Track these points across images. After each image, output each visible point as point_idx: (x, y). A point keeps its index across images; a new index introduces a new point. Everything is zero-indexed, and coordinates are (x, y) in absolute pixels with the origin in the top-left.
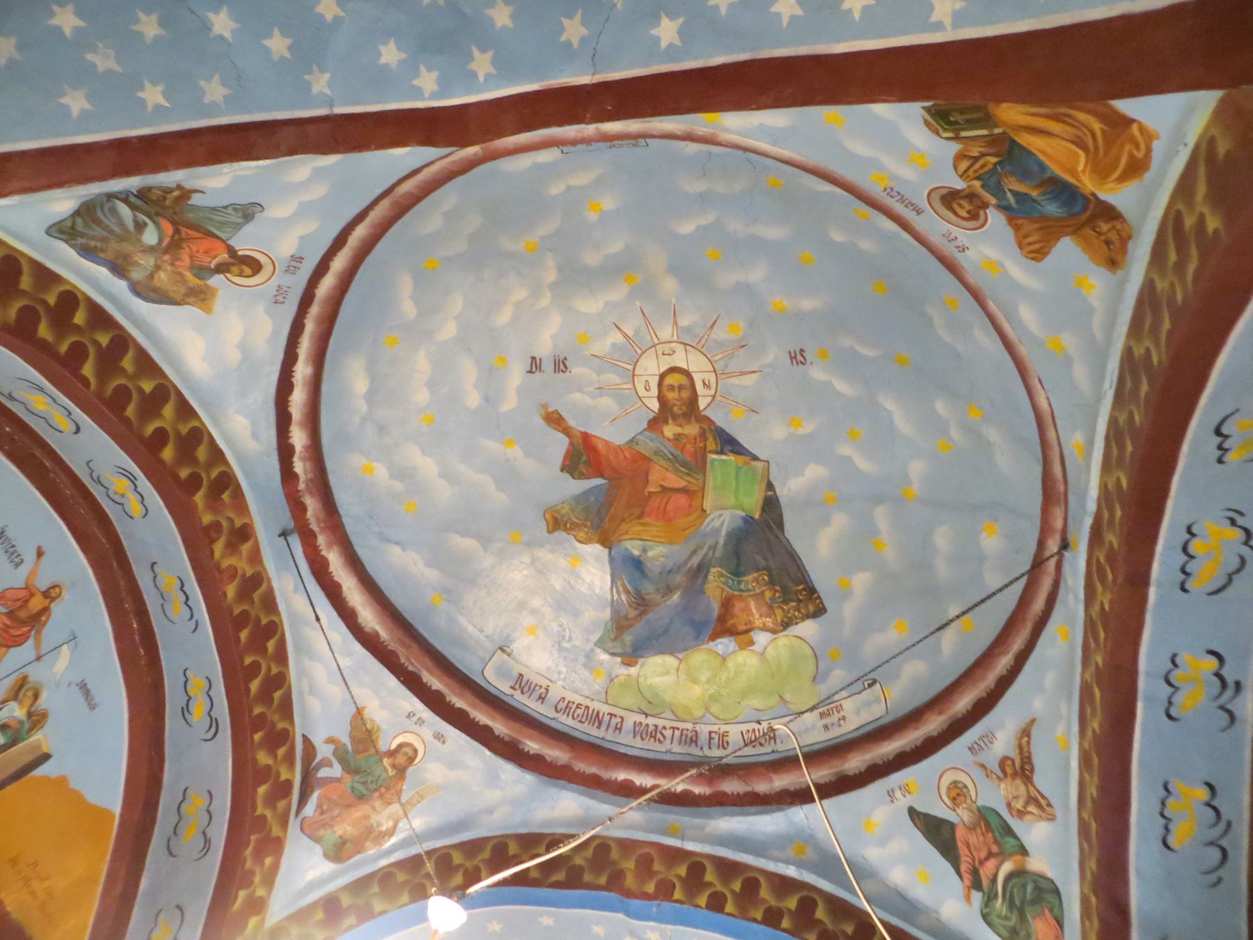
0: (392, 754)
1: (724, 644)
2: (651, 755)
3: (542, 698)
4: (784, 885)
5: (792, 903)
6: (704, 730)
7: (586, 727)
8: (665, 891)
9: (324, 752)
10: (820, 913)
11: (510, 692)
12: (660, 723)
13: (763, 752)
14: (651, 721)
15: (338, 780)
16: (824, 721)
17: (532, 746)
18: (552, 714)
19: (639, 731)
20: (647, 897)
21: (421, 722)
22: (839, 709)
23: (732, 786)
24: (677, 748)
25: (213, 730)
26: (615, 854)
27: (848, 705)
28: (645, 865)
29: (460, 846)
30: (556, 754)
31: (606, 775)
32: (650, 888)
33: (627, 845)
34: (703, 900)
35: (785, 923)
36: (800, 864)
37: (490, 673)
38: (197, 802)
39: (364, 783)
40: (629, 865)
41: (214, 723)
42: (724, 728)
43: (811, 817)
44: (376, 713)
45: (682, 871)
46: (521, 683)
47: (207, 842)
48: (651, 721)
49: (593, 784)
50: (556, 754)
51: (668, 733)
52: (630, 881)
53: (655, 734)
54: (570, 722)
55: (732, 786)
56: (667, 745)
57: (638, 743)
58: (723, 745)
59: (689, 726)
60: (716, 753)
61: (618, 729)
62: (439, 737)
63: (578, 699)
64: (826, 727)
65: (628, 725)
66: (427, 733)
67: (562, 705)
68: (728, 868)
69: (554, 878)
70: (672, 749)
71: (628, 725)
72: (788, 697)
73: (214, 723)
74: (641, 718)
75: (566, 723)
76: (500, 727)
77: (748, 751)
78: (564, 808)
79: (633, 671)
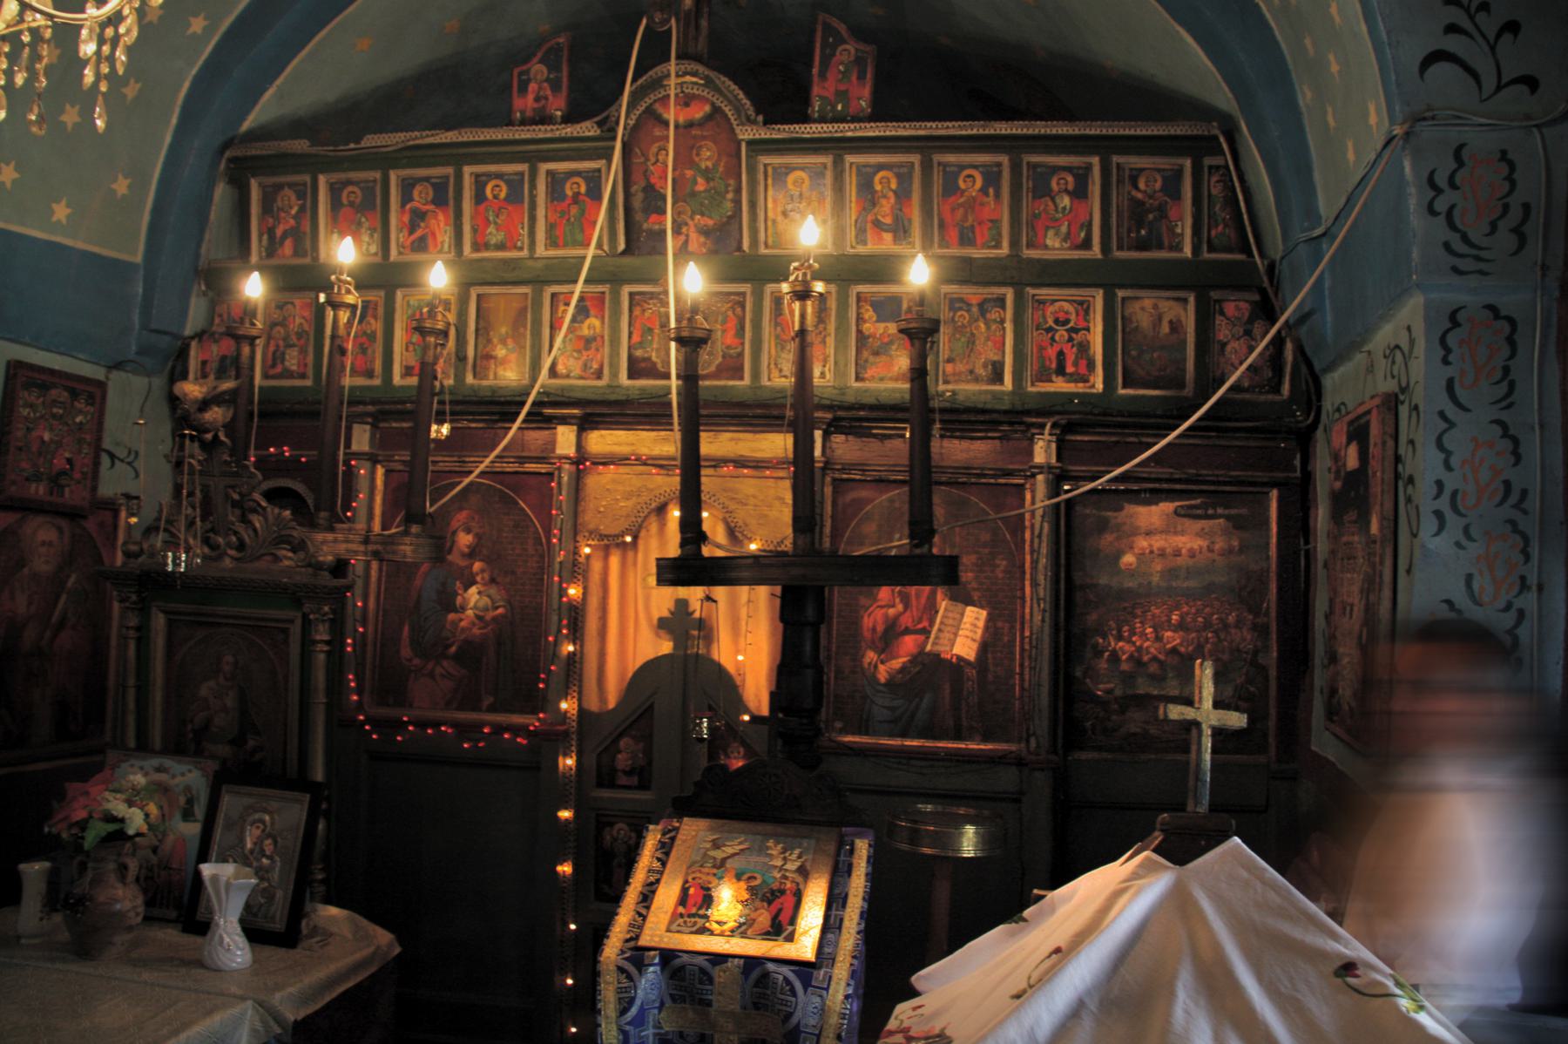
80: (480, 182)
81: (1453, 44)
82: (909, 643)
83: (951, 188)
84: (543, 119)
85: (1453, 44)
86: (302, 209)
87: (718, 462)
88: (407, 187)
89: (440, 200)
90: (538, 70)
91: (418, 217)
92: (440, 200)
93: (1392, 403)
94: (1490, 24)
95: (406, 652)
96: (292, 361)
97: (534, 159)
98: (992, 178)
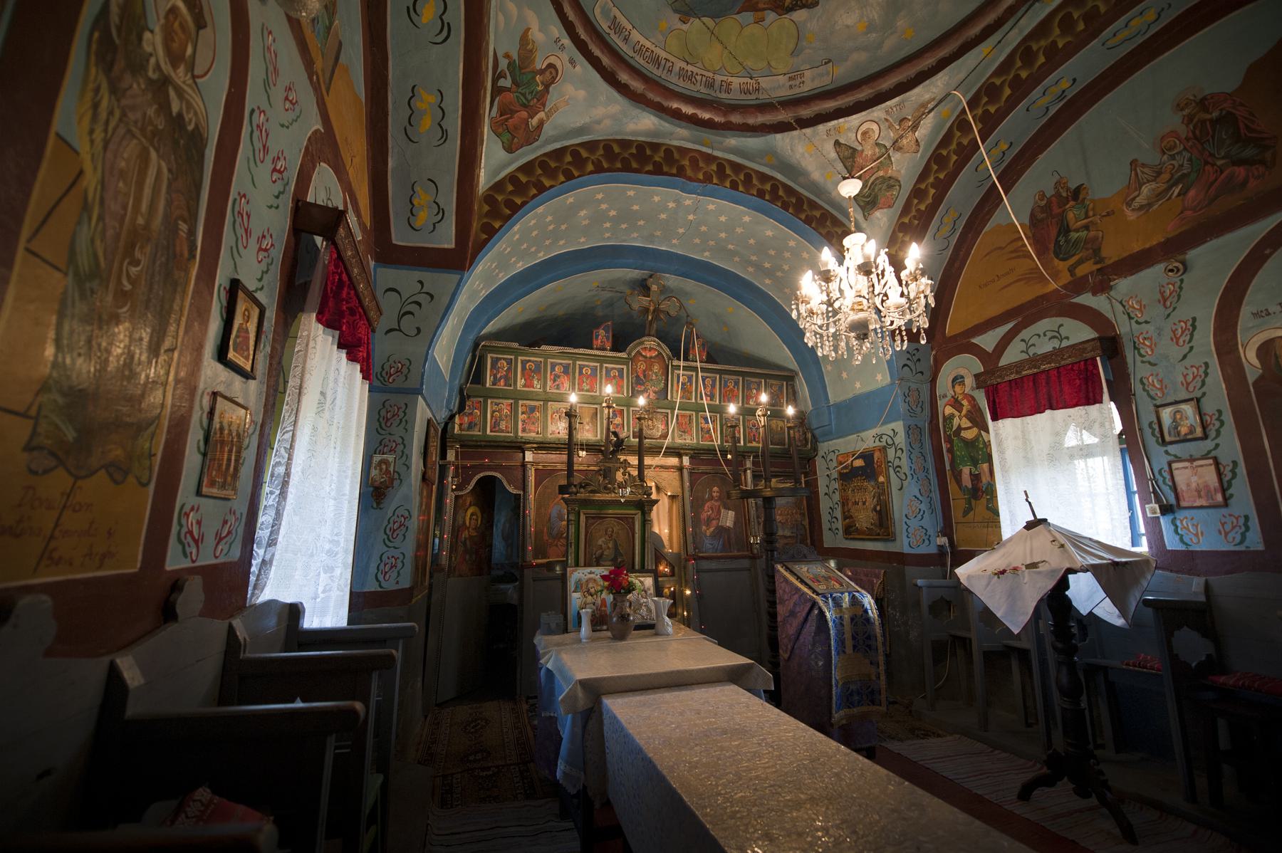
0: (542, 72)
1: (748, 16)
2: (688, 93)
3: (626, 39)
4: (764, 178)
5: (768, 187)
6: (718, 78)
7: (651, 67)
8: (708, 179)
9: (503, 64)
10: (781, 193)
11: (608, 30)
12: (695, 70)
13: (751, 99)
14: (690, 68)
15: (509, 90)
16: (792, 83)
17: (624, 77)
18: (631, 54)
19: (683, 74)
20: (700, 181)
21: (562, 48)
22: (802, 76)
23: (736, 119)
24: (703, 90)
25: (445, 33)
26: (676, 156)
27: (807, 73)
28: (694, 162)
29: (582, 145)
30: (637, 85)
31: (666, 104)
32: (701, 177)
33: (683, 151)
34: (728, 184)
35: (767, 197)
36: (772, 167)
37: (597, 11)
38: (427, 100)
39: (524, 95)
40: (686, 162)
41: (446, 28)
42: (731, 79)
43: (781, 141)
44: (536, 35)
45: (714, 167)
46: (615, 24)
47: (444, 133)
48: (690, 68)
49: (660, 109)
50: (637, 85)
51: (699, 78)
52: (689, 172)
53: (690, 77)
54: (642, 61)
55: (736, 119)
56: (698, 87)
57: (681, 83)
58: (728, 91)
59: (711, 75)
60: (723, 95)
61: (670, 71)
62: (572, 62)
63: (648, 44)
64: (791, 87)
65: (676, 69)
66: (565, 57)
67: (637, 47)
68: (737, 167)
69: (647, 168)
70: (699, 90)
71: (676, 69)
72: (773, 63)
73: (446, 28)
74: (683, 65)
75: (639, 61)
76: (606, 61)
77: (743, 97)
78: (643, 124)
79: (685, 27)
80: (581, 368)
81: (908, 363)
82: (714, 522)
83: (726, 385)
84: (604, 349)
85: (908, 363)
86: (509, 369)
87: (650, 467)
88: (553, 366)
89: (566, 372)
90: (602, 332)
91: (557, 376)
92: (566, 372)
93: (883, 450)
94: (915, 358)
95: (546, 538)
96: (503, 425)
97: (602, 362)
98: (737, 383)
